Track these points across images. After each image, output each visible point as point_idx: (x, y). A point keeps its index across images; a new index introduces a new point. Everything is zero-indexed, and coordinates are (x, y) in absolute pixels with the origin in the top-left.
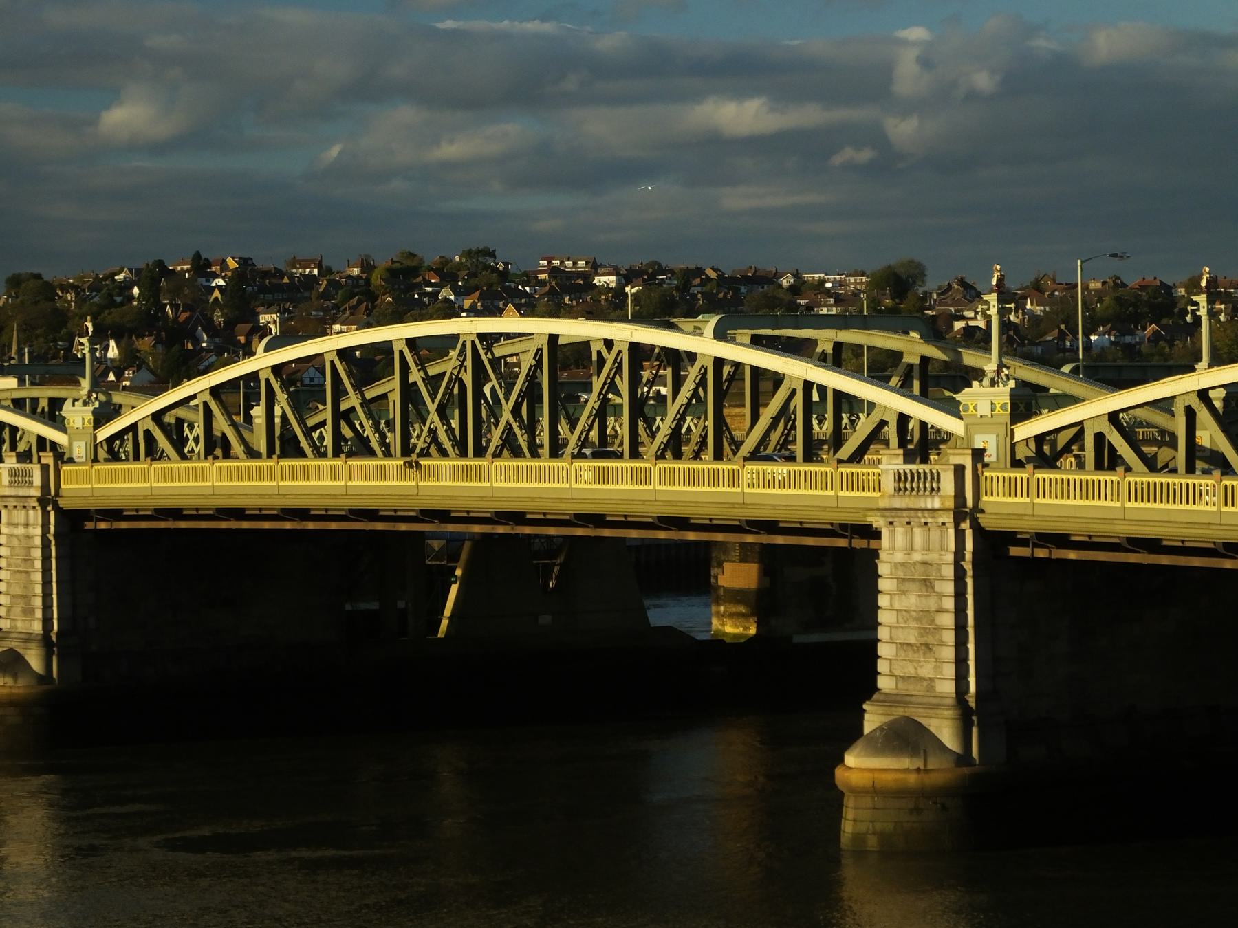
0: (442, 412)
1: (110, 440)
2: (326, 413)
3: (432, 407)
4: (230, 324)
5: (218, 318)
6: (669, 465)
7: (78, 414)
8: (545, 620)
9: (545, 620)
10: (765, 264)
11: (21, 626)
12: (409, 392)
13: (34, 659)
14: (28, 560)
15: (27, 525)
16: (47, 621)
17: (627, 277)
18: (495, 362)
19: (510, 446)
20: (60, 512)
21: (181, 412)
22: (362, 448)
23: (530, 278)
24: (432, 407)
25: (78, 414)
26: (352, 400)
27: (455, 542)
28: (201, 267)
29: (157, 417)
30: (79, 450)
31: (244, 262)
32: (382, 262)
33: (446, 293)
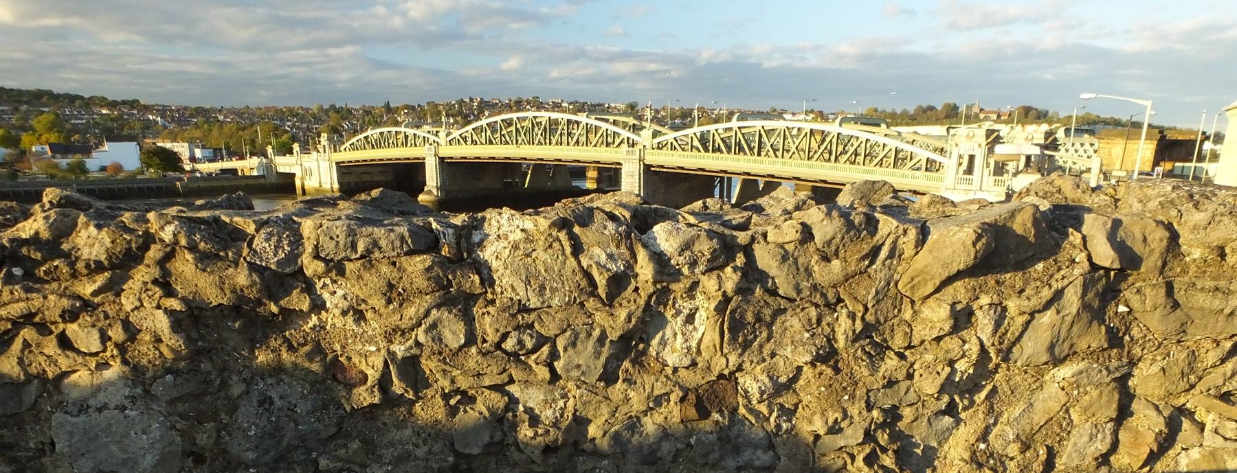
0: (525, 134)
2: (498, 135)
3: (522, 133)
4: (478, 114)
5: (476, 113)
6: (576, 147)
7: (442, 134)
8: (549, 184)
9: (549, 184)
10: (602, 102)
11: (432, 184)
12: (517, 130)
13: (435, 191)
17: (570, 104)
18: (537, 123)
19: (540, 143)
20: (439, 158)
21: (466, 134)
22: (507, 143)
23: (548, 104)
24: (522, 133)
25: (442, 134)
26: (504, 132)
27: (528, 165)
28: (471, 100)
29: (460, 135)
31: (481, 99)
32: (513, 99)
33: (528, 107)
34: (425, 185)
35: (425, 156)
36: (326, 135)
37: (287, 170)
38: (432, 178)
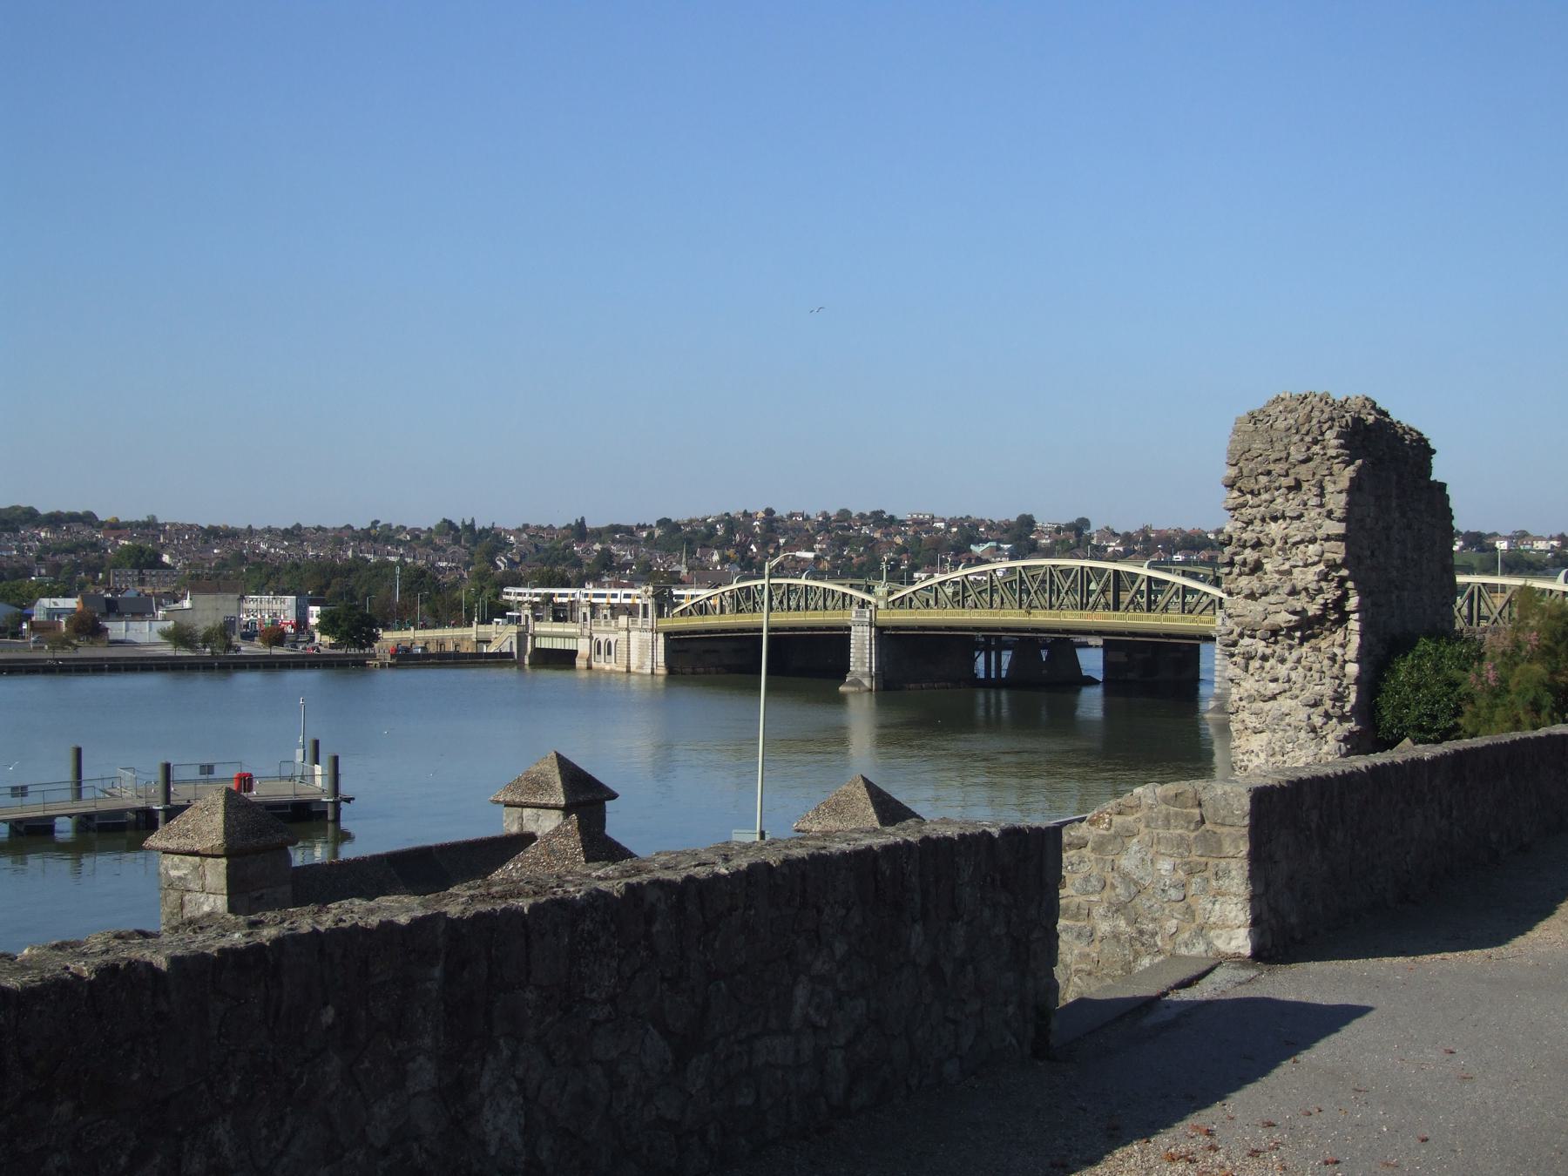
1: (894, 601)
7: (881, 589)
14: (864, 644)
15: (863, 632)
16: (871, 668)
20: (876, 627)
30: (882, 604)
34: (848, 670)
35: (850, 624)
36: (651, 588)
37: (558, 644)
38: (862, 655)
